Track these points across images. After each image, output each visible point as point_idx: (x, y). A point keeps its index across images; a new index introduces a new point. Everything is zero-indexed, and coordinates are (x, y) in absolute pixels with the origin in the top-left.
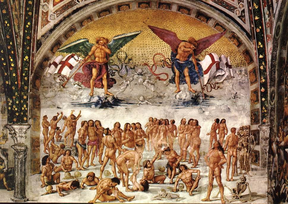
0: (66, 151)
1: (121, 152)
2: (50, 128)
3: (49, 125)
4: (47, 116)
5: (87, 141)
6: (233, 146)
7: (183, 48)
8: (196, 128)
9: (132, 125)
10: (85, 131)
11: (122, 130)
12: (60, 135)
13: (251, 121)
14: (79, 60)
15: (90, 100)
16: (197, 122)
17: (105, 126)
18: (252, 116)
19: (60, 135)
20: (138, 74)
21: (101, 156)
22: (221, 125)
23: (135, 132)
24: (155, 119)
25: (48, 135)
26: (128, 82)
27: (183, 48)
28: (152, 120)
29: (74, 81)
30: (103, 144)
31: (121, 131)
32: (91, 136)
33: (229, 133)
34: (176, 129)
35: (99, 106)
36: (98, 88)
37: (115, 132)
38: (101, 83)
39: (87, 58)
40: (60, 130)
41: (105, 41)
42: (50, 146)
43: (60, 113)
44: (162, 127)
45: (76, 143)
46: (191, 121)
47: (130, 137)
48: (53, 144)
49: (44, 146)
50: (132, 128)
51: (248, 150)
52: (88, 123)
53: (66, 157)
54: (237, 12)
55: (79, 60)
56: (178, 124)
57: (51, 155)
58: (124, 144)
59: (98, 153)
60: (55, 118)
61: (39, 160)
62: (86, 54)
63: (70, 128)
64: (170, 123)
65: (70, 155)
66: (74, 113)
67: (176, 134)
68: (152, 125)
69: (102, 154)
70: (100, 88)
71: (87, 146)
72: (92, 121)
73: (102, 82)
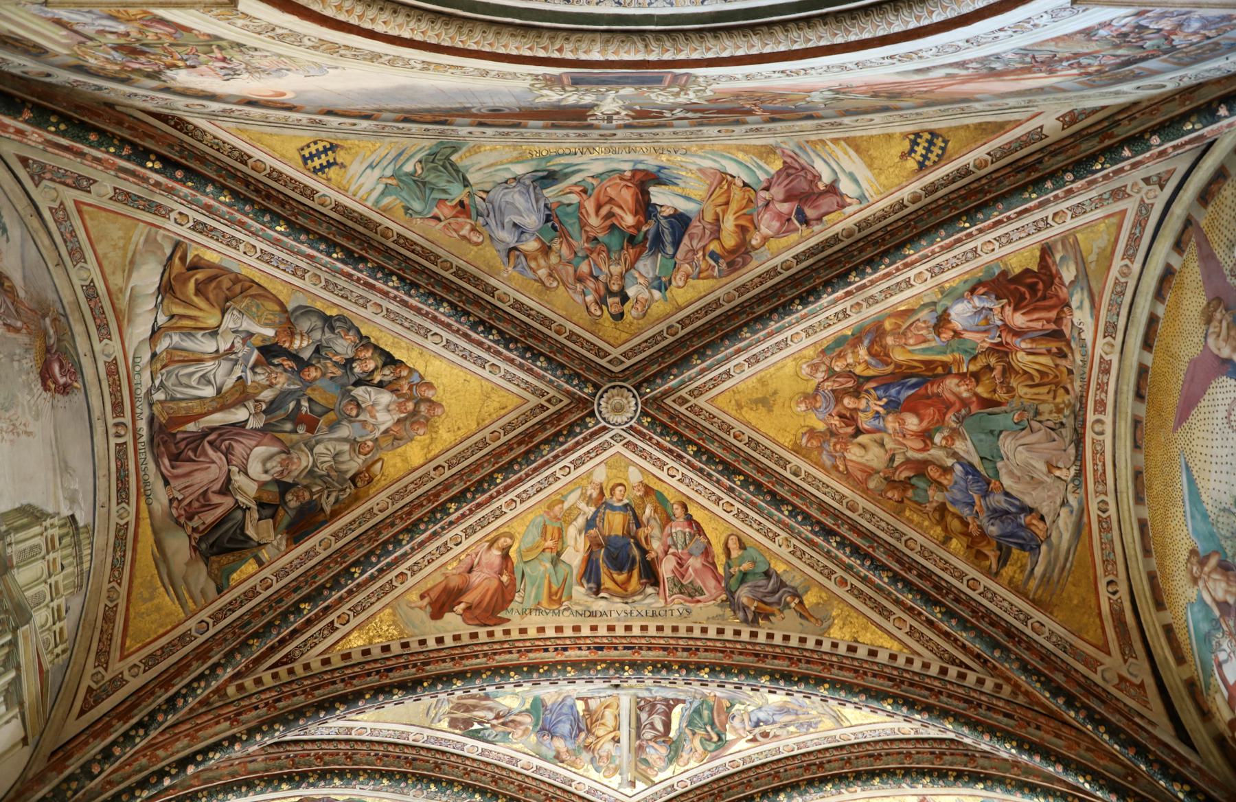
27: (1221, 343)
41: (1194, 560)
54: (1151, 194)
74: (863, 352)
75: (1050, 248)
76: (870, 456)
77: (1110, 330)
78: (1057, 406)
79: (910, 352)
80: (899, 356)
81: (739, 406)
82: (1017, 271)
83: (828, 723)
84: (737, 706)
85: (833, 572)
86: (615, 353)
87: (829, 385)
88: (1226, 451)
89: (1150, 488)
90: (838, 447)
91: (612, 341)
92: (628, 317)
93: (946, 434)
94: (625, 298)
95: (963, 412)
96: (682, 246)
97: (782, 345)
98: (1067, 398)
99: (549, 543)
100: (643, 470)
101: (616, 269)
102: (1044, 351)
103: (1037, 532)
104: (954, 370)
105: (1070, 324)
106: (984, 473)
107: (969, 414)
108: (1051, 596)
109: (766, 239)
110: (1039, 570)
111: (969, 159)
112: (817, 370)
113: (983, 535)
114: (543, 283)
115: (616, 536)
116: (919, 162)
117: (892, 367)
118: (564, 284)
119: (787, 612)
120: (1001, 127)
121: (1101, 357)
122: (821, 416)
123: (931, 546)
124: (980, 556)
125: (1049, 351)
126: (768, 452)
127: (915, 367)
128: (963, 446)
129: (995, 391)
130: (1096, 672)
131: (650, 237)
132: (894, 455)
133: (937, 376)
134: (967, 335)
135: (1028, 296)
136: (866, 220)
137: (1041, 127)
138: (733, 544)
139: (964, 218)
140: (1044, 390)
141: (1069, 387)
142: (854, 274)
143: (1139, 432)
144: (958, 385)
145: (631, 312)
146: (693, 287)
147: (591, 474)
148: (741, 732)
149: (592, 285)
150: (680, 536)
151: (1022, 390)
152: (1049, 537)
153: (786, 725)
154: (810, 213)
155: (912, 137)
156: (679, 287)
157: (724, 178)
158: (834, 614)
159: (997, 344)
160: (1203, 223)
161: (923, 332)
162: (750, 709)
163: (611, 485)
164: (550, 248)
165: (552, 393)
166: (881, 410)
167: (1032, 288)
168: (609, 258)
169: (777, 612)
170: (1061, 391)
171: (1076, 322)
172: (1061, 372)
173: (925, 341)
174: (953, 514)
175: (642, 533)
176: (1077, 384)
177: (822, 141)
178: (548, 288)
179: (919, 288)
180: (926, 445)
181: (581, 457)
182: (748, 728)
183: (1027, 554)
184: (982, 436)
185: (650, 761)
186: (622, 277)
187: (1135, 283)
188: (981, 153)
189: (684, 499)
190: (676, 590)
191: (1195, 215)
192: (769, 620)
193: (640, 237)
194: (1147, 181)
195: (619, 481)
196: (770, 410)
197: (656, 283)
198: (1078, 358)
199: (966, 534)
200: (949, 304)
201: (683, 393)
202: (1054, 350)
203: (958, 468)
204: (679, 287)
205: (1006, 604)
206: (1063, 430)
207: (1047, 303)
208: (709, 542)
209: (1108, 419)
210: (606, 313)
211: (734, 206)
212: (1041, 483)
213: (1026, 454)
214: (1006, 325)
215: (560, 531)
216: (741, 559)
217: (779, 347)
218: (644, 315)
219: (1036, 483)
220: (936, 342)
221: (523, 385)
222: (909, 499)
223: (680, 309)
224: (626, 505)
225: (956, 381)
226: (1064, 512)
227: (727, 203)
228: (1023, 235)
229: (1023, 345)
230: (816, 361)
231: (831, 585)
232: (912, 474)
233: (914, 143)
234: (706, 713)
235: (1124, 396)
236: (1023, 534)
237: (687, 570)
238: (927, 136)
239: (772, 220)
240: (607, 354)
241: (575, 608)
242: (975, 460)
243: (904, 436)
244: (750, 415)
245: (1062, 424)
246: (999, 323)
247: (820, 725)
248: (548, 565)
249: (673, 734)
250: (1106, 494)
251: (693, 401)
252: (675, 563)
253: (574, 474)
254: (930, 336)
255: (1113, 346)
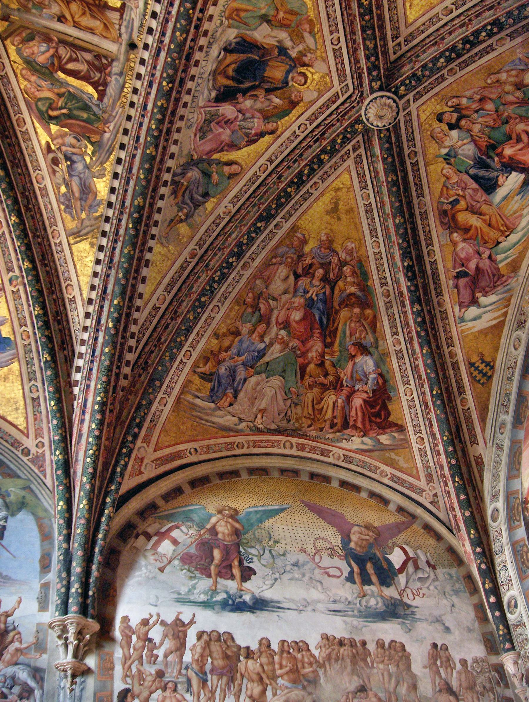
0: (167, 683)
1: (276, 690)
2: (134, 638)
3: (134, 633)
4: (130, 617)
5: (208, 667)
6: (471, 687)
7: (358, 535)
8: (403, 655)
9: (293, 644)
10: (204, 649)
11: (274, 651)
12: (155, 652)
13: (487, 650)
14: (190, 533)
15: (212, 597)
16: (403, 646)
17: (242, 640)
18: (484, 641)
19: (155, 652)
20: (293, 565)
21: (239, 696)
22: (442, 653)
23: (299, 656)
24: (332, 637)
25: (132, 651)
26: (277, 575)
27: (358, 535)
28: (326, 637)
29: (181, 564)
30: (241, 674)
31: (273, 654)
32: (216, 659)
33: (458, 666)
34: (370, 655)
35: (229, 608)
36: (225, 579)
37: (261, 653)
38: (229, 572)
39: (202, 532)
40: (155, 643)
41: (232, 512)
42: (134, 670)
43: (154, 613)
44: (344, 651)
45: (187, 668)
46: (394, 643)
47: (291, 665)
48: (141, 668)
49: (124, 669)
50: (294, 650)
51: (494, 695)
52: (210, 635)
53: (168, 693)
54: (427, 496)
55: (190, 533)
56: (371, 647)
57: (136, 689)
58: (281, 676)
59: (232, 689)
60: (145, 623)
61: (112, 695)
62: (201, 526)
63: (174, 641)
64: (358, 645)
65: (175, 690)
66: (181, 617)
67: (373, 663)
68: (327, 646)
69: (240, 690)
70: (228, 579)
71: (209, 676)
72: (217, 632)
73: (231, 570)
74: (353, 289)
75: (402, 431)
76: (279, 282)
77: (348, 460)
78: (300, 418)
79: (345, 323)
80: (344, 314)
81: (337, 190)
82: (390, 407)
83: (72, 225)
84: (90, 149)
85: (200, 248)
86: (413, 107)
87: (335, 260)
88: (302, 536)
89: (262, 481)
90: (289, 260)
91: (424, 107)
92: (436, 125)
93: (285, 339)
94: (451, 127)
95: (298, 352)
96: (472, 181)
97: (373, 233)
98: (305, 425)
99: (281, 15)
100: (312, 103)
101: (476, 128)
102: (335, 414)
103: (222, 401)
104: (327, 350)
105: (352, 434)
106: (258, 364)
107: (297, 356)
108: (184, 411)
109: (455, 244)
110: (198, 401)
111: (469, 396)
112: (348, 254)
113: (219, 363)
114: (495, 73)
115: (265, 71)
116: (474, 363)
117: (337, 307)
118: (485, 87)
119: (176, 209)
120: (483, 420)
121: (331, 451)
122: (314, 251)
123: (213, 325)
124: (207, 360)
125: (335, 417)
126: (297, 207)
127: (334, 323)
128: (276, 351)
129: (311, 376)
130: (142, 442)
131: (489, 161)
132: (277, 300)
133: (325, 338)
134: (350, 364)
135: (373, 410)
136: (447, 318)
137: (478, 444)
138: (235, 168)
139: (439, 392)
140: (310, 411)
141: (312, 428)
142: (419, 308)
143: (291, 474)
144: (317, 351)
145: (439, 127)
146: (439, 180)
147: (324, 60)
148: (60, 141)
149: (473, 106)
150: (250, 125)
151: (310, 396)
152: (219, 409)
153: (67, 185)
154: (462, 281)
155: (492, 364)
156: (442, 169)
157: (509, 230)
158: (171, 247)
159: (342, 382)
160: (415, 526)
161: (358, 334)
162: (88, 159)
163: (309, 75)
164: (519, 89)
165: (404, 49)
166: (309, 295)
167: (377, 415)
168: (487, 126)
169: (177, 200)
170: (309, 422)
171: (354, 438)
172: (321, 423)
173: (351, 335)
174: (233, 341)
175: (261, 93)
176: (313, 433)
177: (508, 306)
178: (489, 75)
179: (390, 339)
180: (280, 324)
181: (341, 56)
182: (64, 148)
183: (208, 393)
184: (282, 364)
185: (31, 44)
186: (469, 131)
187: (377, 478)
188: (471, 404)
189: (279, 132)
190: (208, 116)
191: (418, 521)
192: (172, 194)
193: (492, 154)
194: (435, 495)
195: (309, 81)
196: (327, 213)
197: (453, 154)
198: (330, 436)
199: (220, 351)
200: (375, 357)
201: (362, 150)
202: (336, 421)
203: (262, 346)
204: (442, 169)
205: (176, 378)
206: (285, 421)
207: (367, 423)
208: (240, 149)
209: (294, 452)
210: (447, 109)
211: (486, 229)
212: (253, 404)
213: (270, 395)
214: (354, 392)
215: (287, 26)
216: (221, 174)
217: (373, 232)
218: (432, 137)
219: (253, 400)
220: (348, 342)
221: (422, 28)
222: (246, 308)
223: (426, 165)
224: (287, 83)
225: (320, 350)
226: (235, 419)
227: (490, 225)
228: (413, 416)
229: (340, 401)
230: (355, 254)
231: (192, 246)
232: (262, 312)
233: (488, 364)
234: (85, 115)
235: (310, 465)
236: (220, 391)
237: (222, 127)
238: (490, 373)
239: (467, 253)
240: (415, 100)
241: (220, 30)
242: (267, 359)
243: (288, 309)
244: (327, 198)
245: (289, 421)
246: (356, 388)
247: (69, 217)
248: (263, 12)
249: (61, 75)
250: (248, 448)
251: (352, 156)
252: (229, 117)
253: (329, 47)
254: (354, 338)
255: (338, 460)
